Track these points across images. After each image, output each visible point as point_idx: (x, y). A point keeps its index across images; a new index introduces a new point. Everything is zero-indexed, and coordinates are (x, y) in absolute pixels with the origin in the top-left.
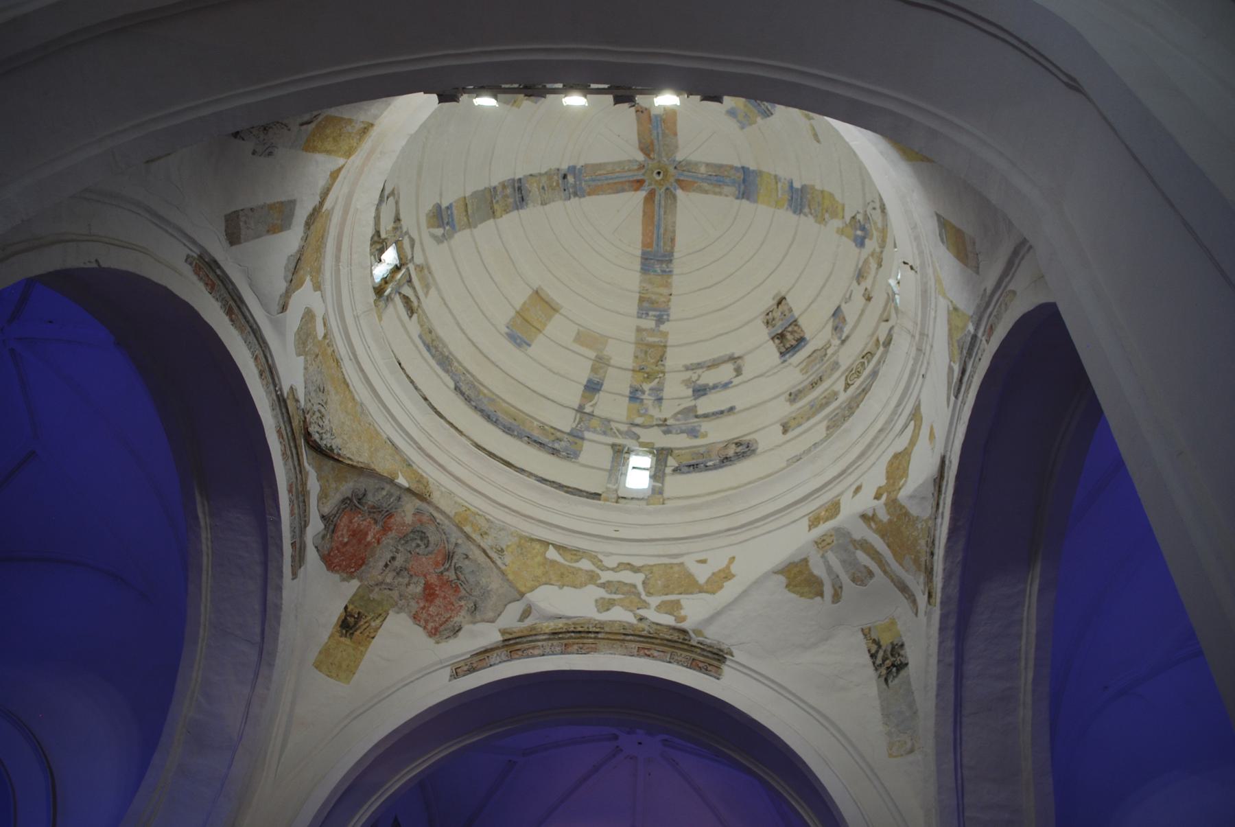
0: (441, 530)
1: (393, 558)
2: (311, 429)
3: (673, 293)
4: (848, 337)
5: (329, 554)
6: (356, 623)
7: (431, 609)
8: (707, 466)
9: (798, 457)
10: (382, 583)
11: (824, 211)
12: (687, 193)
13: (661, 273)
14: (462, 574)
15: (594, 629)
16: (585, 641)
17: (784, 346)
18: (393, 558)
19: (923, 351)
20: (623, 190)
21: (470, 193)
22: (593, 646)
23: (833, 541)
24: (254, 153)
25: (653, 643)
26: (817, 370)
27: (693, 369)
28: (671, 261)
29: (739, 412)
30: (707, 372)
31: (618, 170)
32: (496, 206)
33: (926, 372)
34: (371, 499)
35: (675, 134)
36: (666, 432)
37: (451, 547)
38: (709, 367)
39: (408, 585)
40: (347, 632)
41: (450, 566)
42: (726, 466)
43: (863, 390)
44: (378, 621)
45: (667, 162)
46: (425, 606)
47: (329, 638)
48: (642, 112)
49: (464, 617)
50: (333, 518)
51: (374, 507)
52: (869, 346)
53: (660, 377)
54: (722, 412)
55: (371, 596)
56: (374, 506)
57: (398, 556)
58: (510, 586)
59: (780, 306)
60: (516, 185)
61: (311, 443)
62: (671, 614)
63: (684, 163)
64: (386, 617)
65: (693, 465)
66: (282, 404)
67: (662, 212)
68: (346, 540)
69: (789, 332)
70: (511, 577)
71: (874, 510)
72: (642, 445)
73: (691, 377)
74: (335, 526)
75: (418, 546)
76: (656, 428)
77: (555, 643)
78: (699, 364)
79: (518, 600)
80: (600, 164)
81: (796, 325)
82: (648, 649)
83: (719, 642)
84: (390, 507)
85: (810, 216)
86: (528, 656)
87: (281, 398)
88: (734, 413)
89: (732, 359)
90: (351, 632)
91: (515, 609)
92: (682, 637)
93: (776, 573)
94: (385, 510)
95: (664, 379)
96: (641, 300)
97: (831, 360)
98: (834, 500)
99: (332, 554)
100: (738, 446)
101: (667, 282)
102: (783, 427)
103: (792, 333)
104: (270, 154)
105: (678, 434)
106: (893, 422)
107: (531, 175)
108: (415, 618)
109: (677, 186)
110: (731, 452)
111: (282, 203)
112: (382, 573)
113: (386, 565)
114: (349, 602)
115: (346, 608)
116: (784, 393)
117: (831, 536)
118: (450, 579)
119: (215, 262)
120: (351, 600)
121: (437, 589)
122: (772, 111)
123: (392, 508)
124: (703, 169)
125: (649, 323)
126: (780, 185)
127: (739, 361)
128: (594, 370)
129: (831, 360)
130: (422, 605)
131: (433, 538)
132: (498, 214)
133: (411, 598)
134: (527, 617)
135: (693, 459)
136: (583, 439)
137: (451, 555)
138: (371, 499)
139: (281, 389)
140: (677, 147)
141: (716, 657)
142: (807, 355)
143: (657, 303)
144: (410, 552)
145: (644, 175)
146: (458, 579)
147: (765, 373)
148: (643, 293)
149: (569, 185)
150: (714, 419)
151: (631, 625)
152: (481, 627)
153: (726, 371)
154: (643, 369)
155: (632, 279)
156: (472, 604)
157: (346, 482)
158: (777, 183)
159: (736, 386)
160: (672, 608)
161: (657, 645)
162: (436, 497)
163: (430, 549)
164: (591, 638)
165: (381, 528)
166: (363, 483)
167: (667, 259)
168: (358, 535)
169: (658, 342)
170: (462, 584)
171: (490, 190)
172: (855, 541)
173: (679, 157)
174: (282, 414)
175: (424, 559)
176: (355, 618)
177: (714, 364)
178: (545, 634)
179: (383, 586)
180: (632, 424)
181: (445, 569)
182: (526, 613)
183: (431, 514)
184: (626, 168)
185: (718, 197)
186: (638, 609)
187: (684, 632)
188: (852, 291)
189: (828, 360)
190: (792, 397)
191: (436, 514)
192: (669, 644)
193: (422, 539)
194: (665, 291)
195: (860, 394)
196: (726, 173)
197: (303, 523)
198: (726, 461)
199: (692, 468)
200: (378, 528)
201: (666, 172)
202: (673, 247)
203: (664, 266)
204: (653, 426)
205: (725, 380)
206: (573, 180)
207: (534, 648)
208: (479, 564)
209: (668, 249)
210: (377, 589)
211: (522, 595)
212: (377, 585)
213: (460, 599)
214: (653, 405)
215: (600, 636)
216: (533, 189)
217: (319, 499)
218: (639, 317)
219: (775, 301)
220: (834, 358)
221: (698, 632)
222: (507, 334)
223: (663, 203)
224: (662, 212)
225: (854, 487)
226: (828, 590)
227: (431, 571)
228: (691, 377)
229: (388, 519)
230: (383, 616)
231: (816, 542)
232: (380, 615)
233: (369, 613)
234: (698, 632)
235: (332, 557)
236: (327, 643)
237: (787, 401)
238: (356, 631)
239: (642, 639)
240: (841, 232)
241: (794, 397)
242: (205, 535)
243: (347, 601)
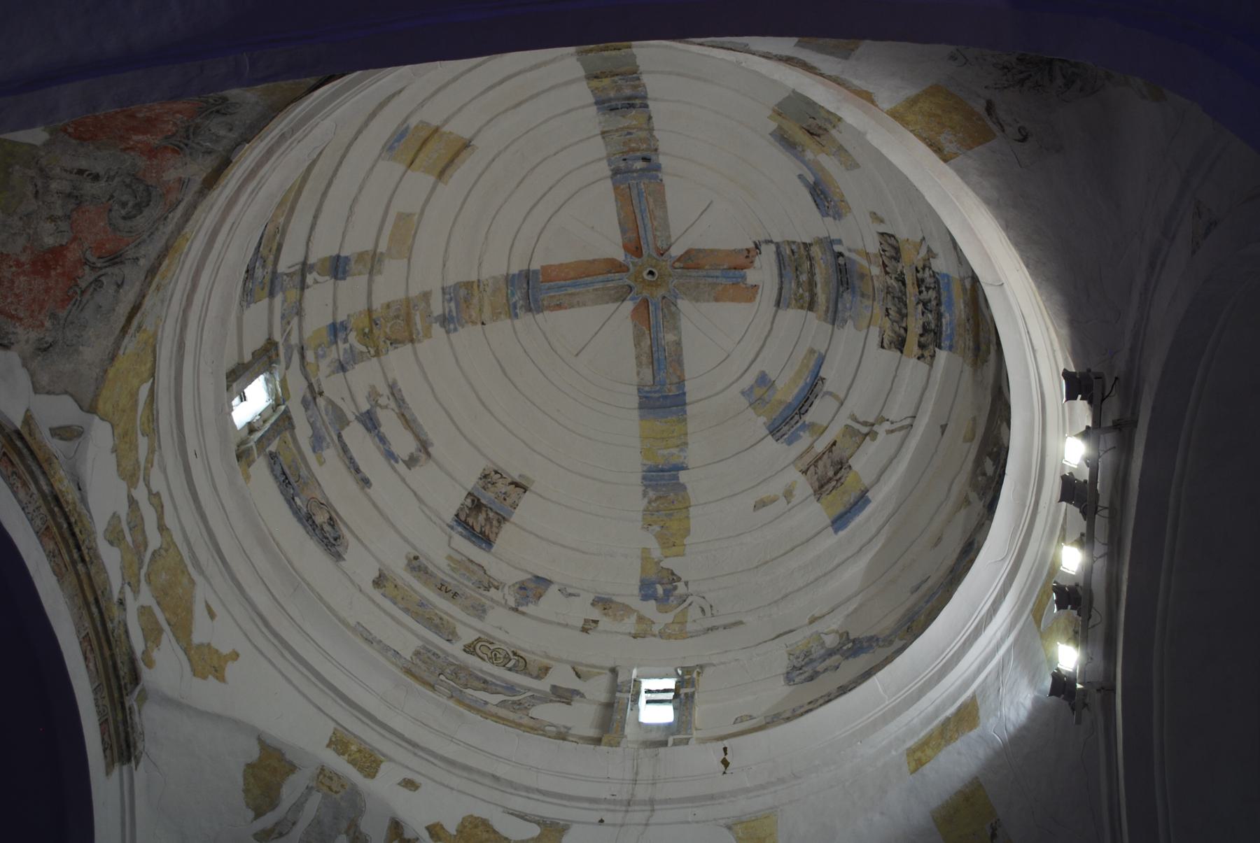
1: (96, 177)
3: (486, 327)
4: (523, 613)
7: (22, 278)
8: (293, 499)
9: (370, 638)
11: (662, 524)
12: (630, 316)
13: (511, 302)
14: (92, 294)
15: (85, 551)
16: (64, 551)
17: (468, 516)
18: (96, 177)
19: (630, 809)
20: (623, 232)
21: (635, 53)
22: (64, 569)
23: (336, 792)
25: (101, 648)
26: (463, 584)
27: (393, 394)
28: (529, 310)
29: (367, 495)
30: (395, 416)
31: (655, 224)
32: (606, 82)
33: (608, 825)
35: (717, 300)
36: (305, 403)
37: (131, 254)
38: (403, 415)
39: (52, 219)
42: (305, 527)
43: (485, 682)
45: (671, 286)
46: (23, 264)
48: (747, 257)
49: (27, 341)
52: (534, 657)
53: (369, 352)
54: (358, 470)
56: (200, 128)
57: (103, 183)
58: (97, 379)
59: (513, 486)
60: (638, 102)
62: (146, 640)
63: (673, 309)
65: (287, 478)
67: (597, 286)
68: (140, 115)
69: (487, 515)
70: (111, 373)
71: (417, 839)
72: (283, 382)
73: (381, 396)
75: (124, 205)
76: (305, 384)
77: (44, 510)
78: (403, 400)
79: (81, 408)
80: (664, 202)
81: (499, 522)
82: (92, 649)
83: (143, 733)
84: (194, 145)
85: (646, 500)
86: (11, 486)
88: (363, 488)
89: (424, 446)
91: (58, 410)
92: (127, 680)
93: (261, 741)
94: (190, 142)
95: (369, 359)
96: (468, 285)
97: (483, 600)
98: (376, 752)
100: (330, 524)
101: (500, 313)
102: (380, 576)
103: (488, 519)
105: (309, 421)
106: (513, 791)
107: (650, 118)
109: (638, 301)
110: (321, 518)
112: (66, 171)
113: (81, 172)
116: (415, 548)
117: (343, 786)
121: (59, 270)
122: (782, 440)
124: (670, 337)
125: (437, 307)
126: (675, 450)
127: (423, 456)
128: (361, 256)
129: (483, 600)
130: (23, 259)
131: (140, 221)
132: (595, 83)
133: (28, 234)
134: (62, 439)
135: (290, 467)
136: (272, 295)
140: (697, 300)
141: (124, 747)
142: (472, 558)
143: (468, 307)
144: (112, 197)
145: (649, 255)
146: (83, 292)
147: (426, 505)
148: (479, 286)
149: (630, 162)
150: (345, 463)
151: (110, 599)
152: (23, 377)
153: (404, 444)
154: (377, 324)
155: (496, 266)
156: (50, 340)
158: (678, 446)
159: (393, 468)
160: (153, 633)
161: (102, 654)
164: (71, 557)
165: (156, 146)
167: (532, 305)
169: (417, 329)
171: (636, 73)
172: (356, 826)
173: (684, 304)
175: (102, 224)
177: (409, 422)
178: (52, 486)
180: (302, 348)
181: (94, 263)
182: (68, 433)
183: (180, 202)
184: (658, 233)
185: (634, 361)
186: (129, 584)
187: (136, 678)
188: (579, 595)
189: (481, 594)
190: (415, 563)
192: (111, 670)
194: (487, 315)
195: (478, 678)
196: (671, 370)
198: (307, 520)
199: (283, 478)
201: (655, 285)
202: (549, 308)
203: (521, 302)
204: (307, 378)
205: (395, 449)
206: (638, 168)
207: (25, 484)
208: (114, 310)
209: (545, 303)
211: (92, 409)
212: (41, 170)
213: (53, 316)
214: (332, 362)
215: (80, 567)
216: (632, 119)
218: (443, 289)
219: (518, 480)
220: (488, 603)
221: (143, 697)
222: (407, 128)
223: (610, 285)
224: (597, 286)
225: (410, 775)
226: (269, 820)
227: (86, 245)
228: (381, 396)
231: (323, 769)
237: (407, 557)
239: (100, 628)
240: (645, 556)
241: (416, 565)
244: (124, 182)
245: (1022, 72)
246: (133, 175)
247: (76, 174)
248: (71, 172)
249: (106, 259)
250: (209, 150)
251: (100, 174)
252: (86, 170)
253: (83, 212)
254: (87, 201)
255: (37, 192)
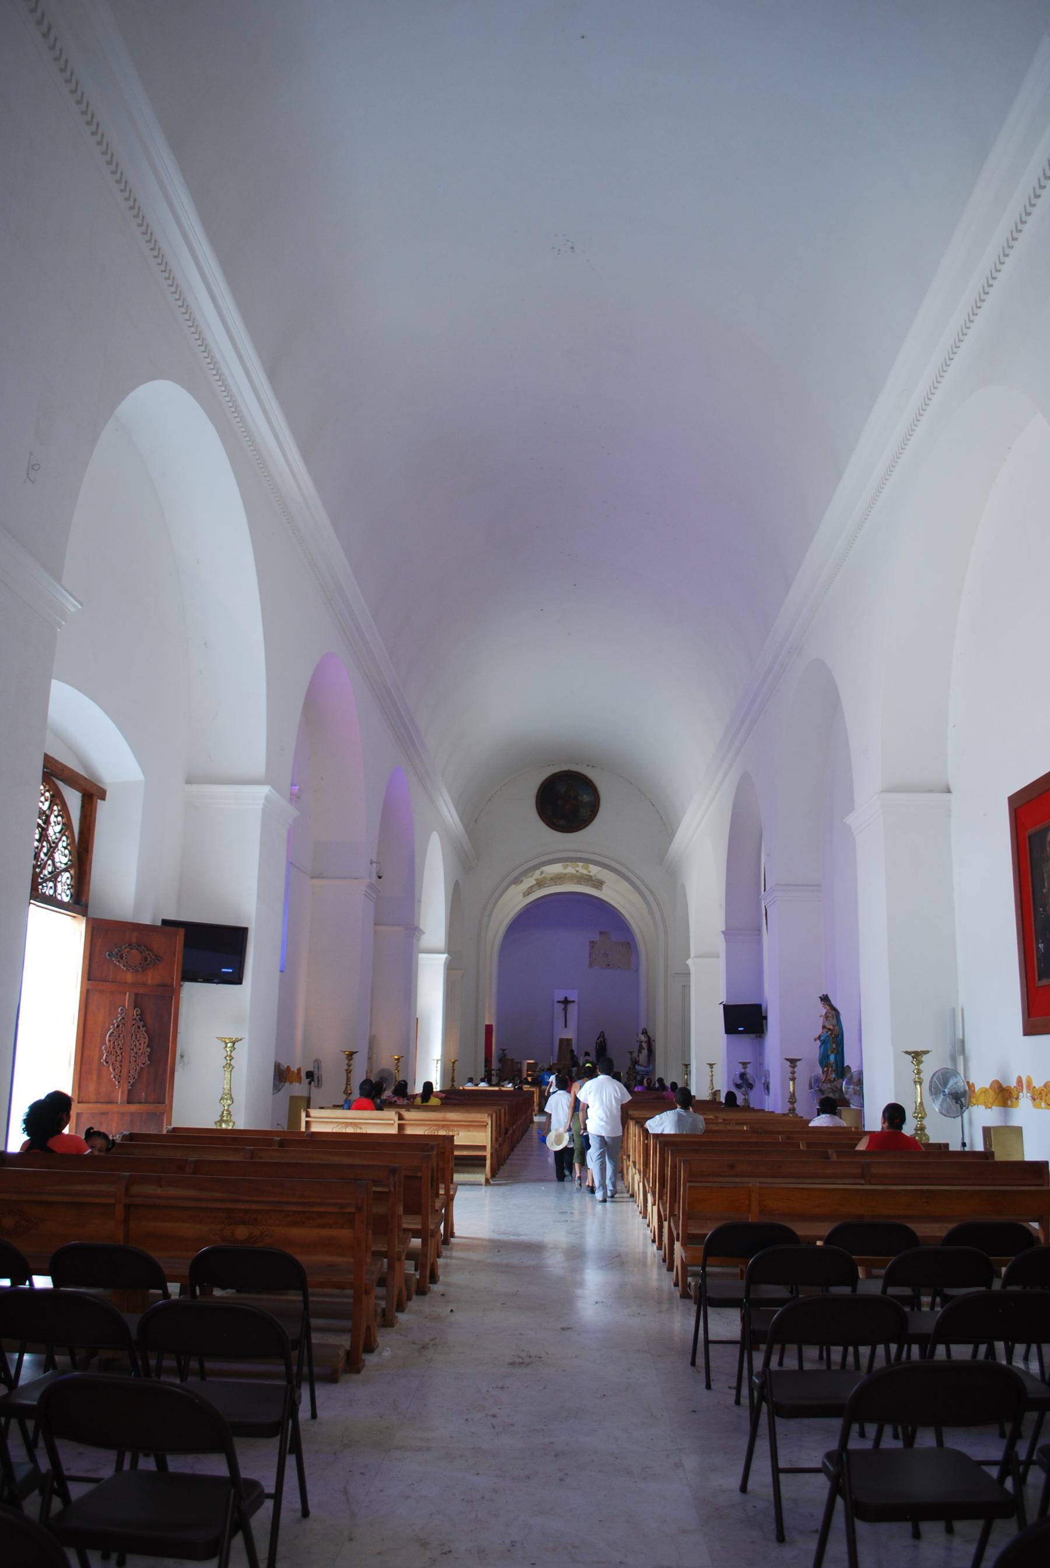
62: (586, 869)
151: (574, 874)
152: (529, 879)
182: (542, 873)
187: (591, 876)
221: (595, 876)
234: (595, 876)
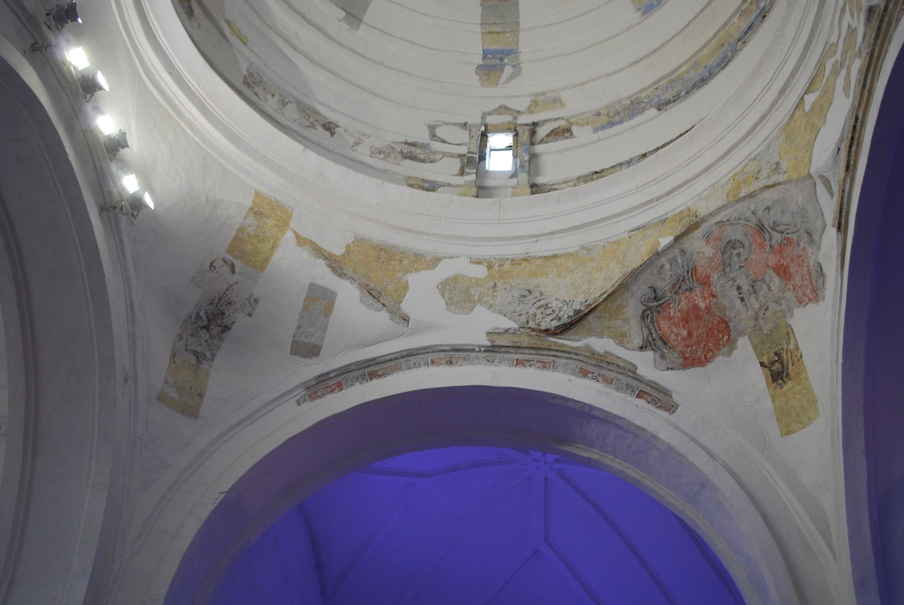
0: (734, 222)
1: (739, 288)
2: (543, 328)
5: (685, 358)
6: (782, 364)
10: (757, 314)
18: (739, 288)
24: (250, 315)
34: (663, 285)
40: (782, 379)
41: (769, 233)
44: (792, 340)
47: (773, 401)
50: (652, 337)
51: (674, 285)
55: (765, 331)
61: (557, 332)
64: (792, 330)
66: (496, 349)
68: (685, 333)
74: (661, 338)
75: (739, 255)
84: (685, 266)
87: (490, 349)
90: (785, 374)
99: (687, 355)
104: (256, 301)
108: (800, 302)
111: (307, 298)
112: (747, 308)
113: (742, 300)
114: (758, 359)
115: (762, 364)
118: (780, 242)
119: (320, 376)
120: (757, 354)
123: (688, 265)
130: (791, 288)
133: (783, 294)
137: (760, 225)
138: (663, 285)
139: (480, 346)
144: (741, 267)
146: (782, 233)
157: (626, 307)
162: (704, 209)
163: (746, 244)
166: (641, 289)
168: (692, 315)
170: (787, 231)
174: (506, 352)
176: (778, 361)
179: (761, 314)
181: (769, 241)
191: (718, 218)
193: (734, 248)
197: (630, 374)
200: (698, 291)
208: (778, 200)
210: (761, 322)
211: (809, 176)
212: (756, 320)
217: (621, 344)
222: (643, 14)
227: (766, 255)
229: (695, 275)
230: (790, 333)
232: (788, 333)
233: (781, 344)
235: (691, 356)
236: (775, 407)
238: (787, 369)
242: (608, 460)
243: (757, 359)
244: (730, 270)
245: (221, 305)
246: (724, 271)
247: (745, 301)
248: (746, 304)
249: (763, 233)
250: (682, 253)
251: (736, 288)
252: (740, 298)
253: (756, 275)
254: (751, 279)
255: (766, 310)
